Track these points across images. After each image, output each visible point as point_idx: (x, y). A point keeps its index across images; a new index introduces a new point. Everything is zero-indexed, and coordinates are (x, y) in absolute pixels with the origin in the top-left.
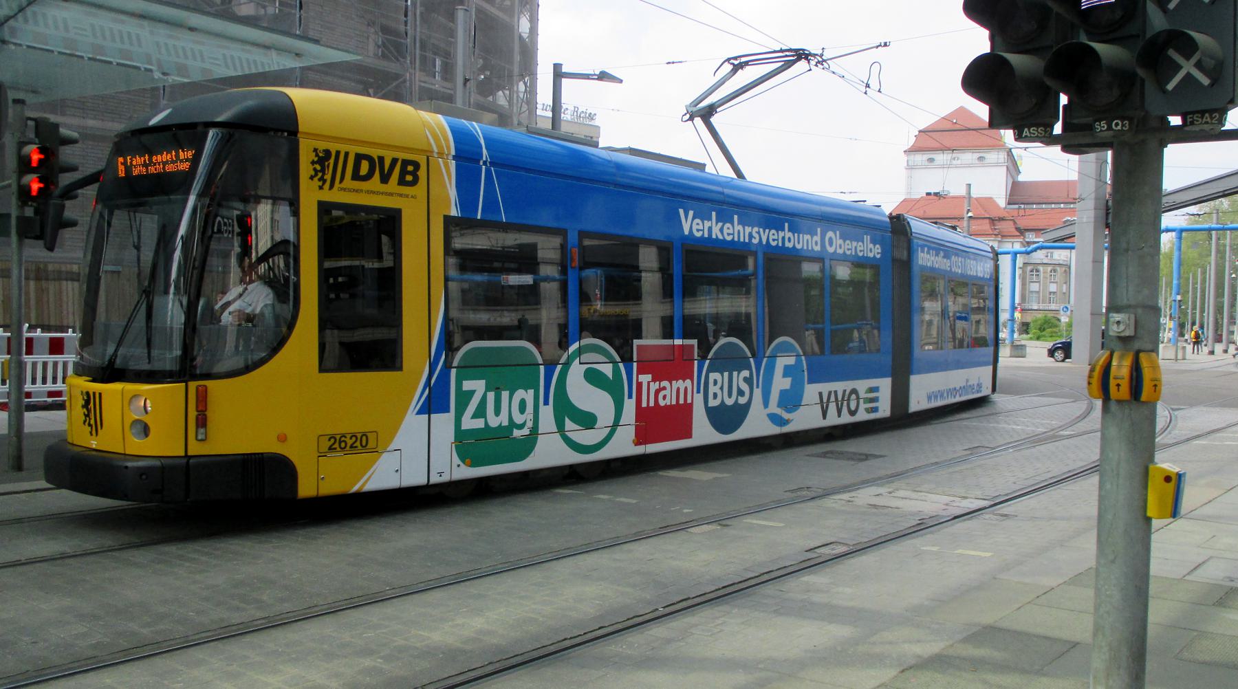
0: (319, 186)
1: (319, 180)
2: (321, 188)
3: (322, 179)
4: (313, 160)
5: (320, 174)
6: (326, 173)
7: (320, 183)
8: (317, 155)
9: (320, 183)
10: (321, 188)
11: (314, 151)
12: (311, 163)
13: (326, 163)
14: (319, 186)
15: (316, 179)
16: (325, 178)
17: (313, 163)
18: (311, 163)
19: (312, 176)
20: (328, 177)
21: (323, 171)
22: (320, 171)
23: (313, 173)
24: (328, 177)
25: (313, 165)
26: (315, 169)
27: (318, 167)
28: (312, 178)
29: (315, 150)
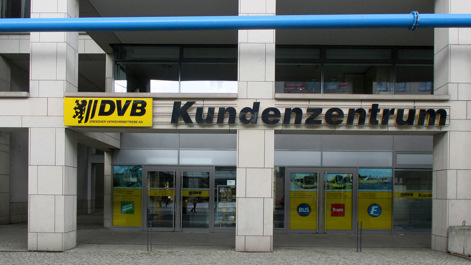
0: (79, 121)
1: (79, 118)
2: (80, 122)
3: (82, 118)
4: (75, 107)
5: (79, 115)
6: (83, 113)
7: (80, 119)
8: (78, 104)
9: (80, 119)
10: (80, 122)
11: (76, 102)
12: (74, 109)
13: (83, 108)
14: (79, 121)
15: (77, 117)
16: (82, 116)
17: (75, 108)
18: (74, 109)
19: (74, 115)
20: (84, 116)
21: (81, 113)
22: (79, 113)
23: (75, 114)
24: (84, 116)
25: (75, 110)
26: (76, 112)
27: (78, 111)
28: (74, 117)
29: (77, 102)
